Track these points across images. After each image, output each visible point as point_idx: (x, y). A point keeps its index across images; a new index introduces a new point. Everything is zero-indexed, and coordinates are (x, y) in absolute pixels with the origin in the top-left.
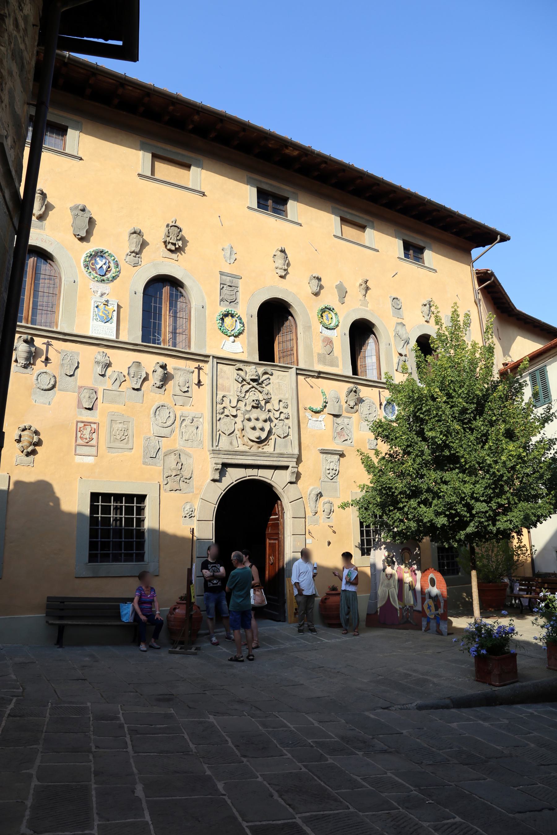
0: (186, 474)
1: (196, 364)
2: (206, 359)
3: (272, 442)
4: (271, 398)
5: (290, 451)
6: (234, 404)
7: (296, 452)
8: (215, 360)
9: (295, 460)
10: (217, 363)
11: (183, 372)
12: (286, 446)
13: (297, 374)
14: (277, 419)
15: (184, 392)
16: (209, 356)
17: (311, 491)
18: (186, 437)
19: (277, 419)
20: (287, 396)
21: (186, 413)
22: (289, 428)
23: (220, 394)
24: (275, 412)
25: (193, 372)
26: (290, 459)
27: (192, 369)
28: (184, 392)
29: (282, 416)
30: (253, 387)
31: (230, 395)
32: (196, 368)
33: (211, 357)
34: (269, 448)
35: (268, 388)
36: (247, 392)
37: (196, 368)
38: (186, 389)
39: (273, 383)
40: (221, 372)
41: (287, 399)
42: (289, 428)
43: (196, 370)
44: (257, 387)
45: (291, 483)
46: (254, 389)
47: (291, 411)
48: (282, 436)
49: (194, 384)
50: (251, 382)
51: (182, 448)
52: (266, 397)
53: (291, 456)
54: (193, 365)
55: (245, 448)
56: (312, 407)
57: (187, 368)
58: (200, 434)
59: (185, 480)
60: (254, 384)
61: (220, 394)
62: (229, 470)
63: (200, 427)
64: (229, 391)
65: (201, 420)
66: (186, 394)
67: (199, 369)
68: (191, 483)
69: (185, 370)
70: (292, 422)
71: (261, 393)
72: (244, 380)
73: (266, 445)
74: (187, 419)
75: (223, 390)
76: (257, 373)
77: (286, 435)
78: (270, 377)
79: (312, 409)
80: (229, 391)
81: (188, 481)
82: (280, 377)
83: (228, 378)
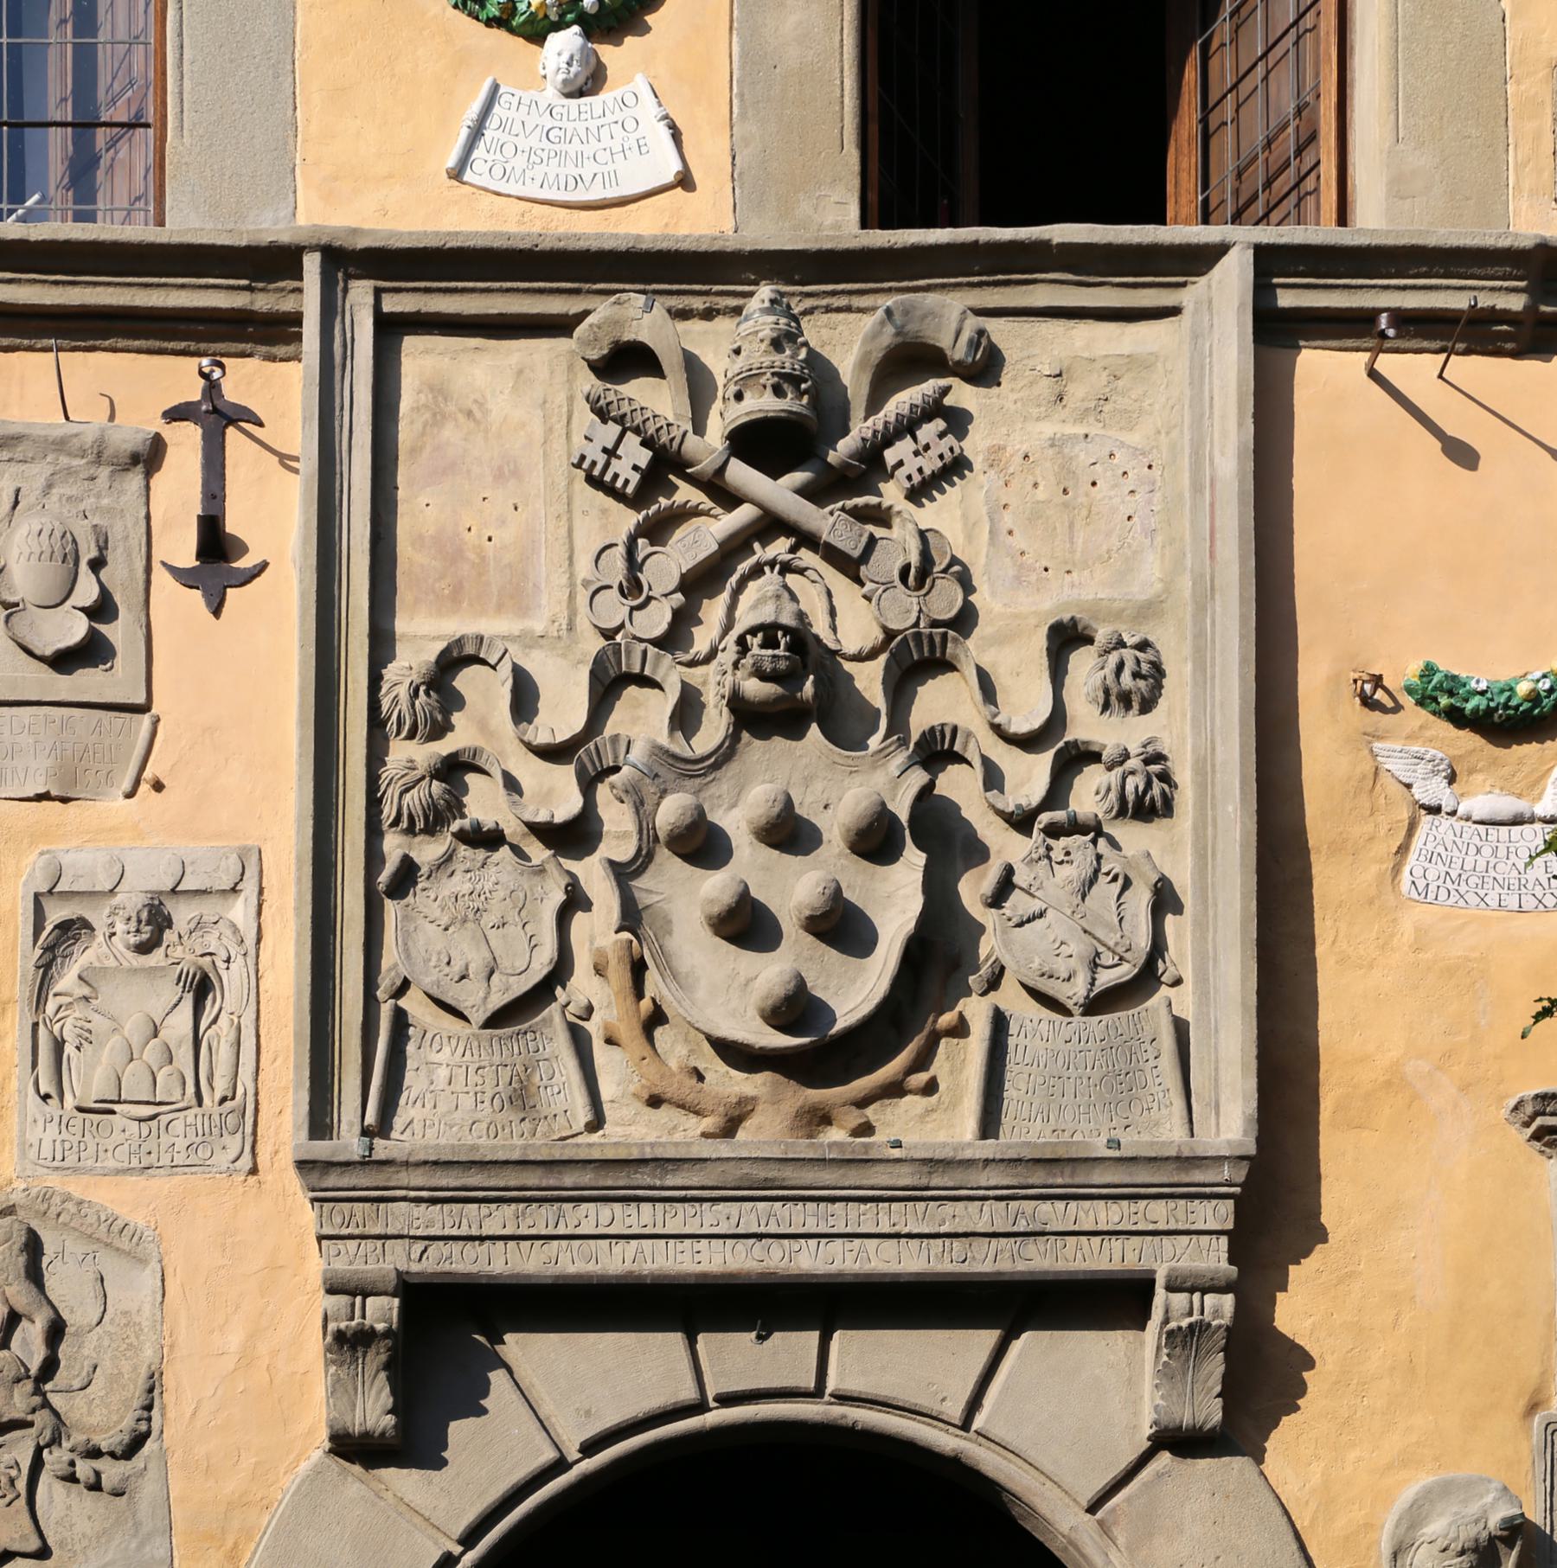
0: (97, 1412)
1: (179, 378)
2: (263, 302)
3: (961, 1065)
4: (965, 620)
5: (1169, 1133)
6: (563, 715)
7: (1230, 1123)
8: (360, 293)
9: (1220, 1214)
10: (390, 329)
11: (38, 473)
12: (1122, 1086)
13: (1276, 332)
14: (1022, 822)
15: (64, 661)
16: (275, 262)
17: (1415, 1516)
18: (89, 1077)
19: (1022, 822)
20: (1149, 577)
21: (85, 864)
22: (1165, 900)
23: (421, 636)
24: (1009, 759)
25: (150, 457)
26: (1159, 1213)
27: (140, 420)
28: (64, 661)
29: (1089, 794)
30: (771, 525)
31: (532, 641)
32: (175, 415)
33: (312, 264)
34: (934, 1120)
35: (944, 516)
36: (701, 582)
37: (175, 415)
38: (75, 629)
39: (995, 455)
40: (438, 418)
41: (1148, 610)
42: (1165, 900)
43: (186, 442)
44: (828, 521)
45: (1178, 1441)
46: (780, 547)
47: (1199, 723)
48: (1076, 991)
49: (163, 582)
50: (741, 474)
51: (54, 1181)
52: (903, 610)
53: (1176, 1175)
54: (139, 388)
55: (681, 1133)
56: (1447, 665)
57: (89, 418)
58: (224, 1054)
59: (84, 1469)
60: (780, 492)
61: (421, 636)
62: (524, 1350)
63: (233, 980)
64: (516, 598)
65: (240, 911)
66: (87, 682)
67: (217, 417)
68: (148, 1490)
69: (61, 445)
70: (1205, 849)
71: (850, 566)
72: (666, 464)
73: (895, 1090)
74: (98, 917)
75: (454, 599)
76: (786, 360)
77: (1125, 972)
78: (963, 395)
79: (1453, 685)
80: (516, 598)
81: (112, 1472)
82: (1077, 392)
83: (508, 472)
